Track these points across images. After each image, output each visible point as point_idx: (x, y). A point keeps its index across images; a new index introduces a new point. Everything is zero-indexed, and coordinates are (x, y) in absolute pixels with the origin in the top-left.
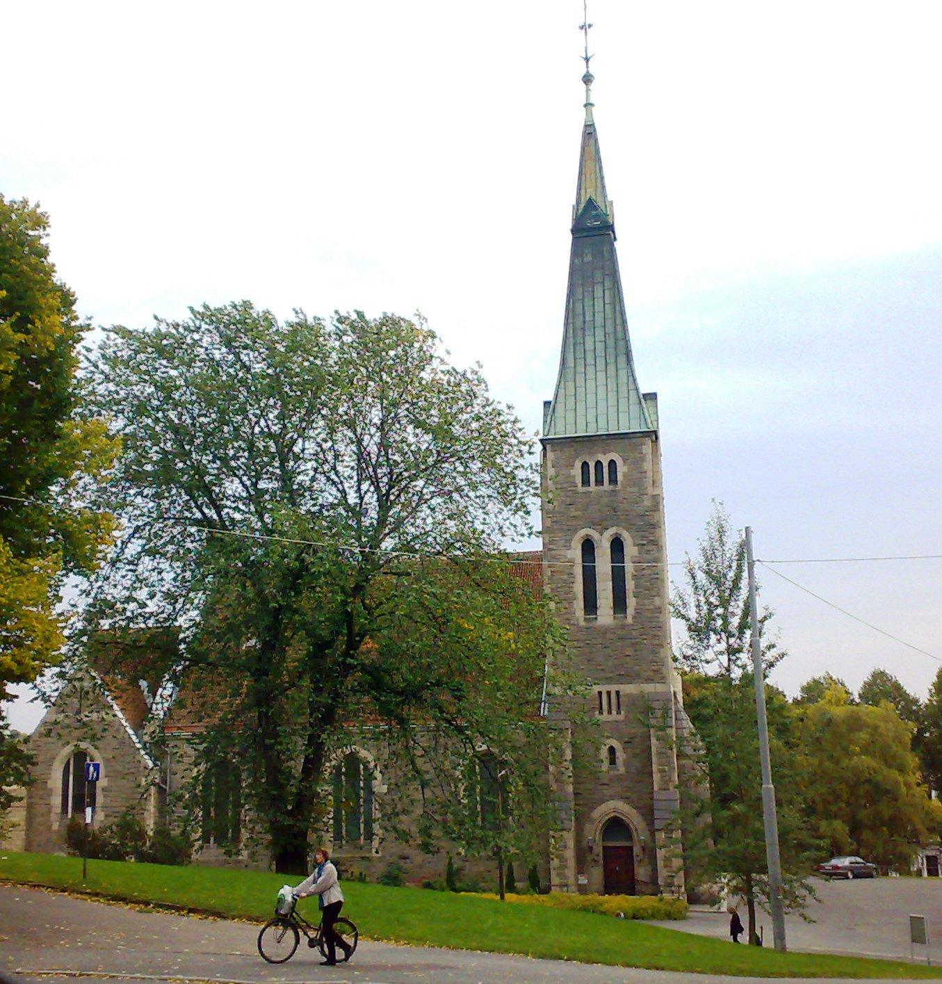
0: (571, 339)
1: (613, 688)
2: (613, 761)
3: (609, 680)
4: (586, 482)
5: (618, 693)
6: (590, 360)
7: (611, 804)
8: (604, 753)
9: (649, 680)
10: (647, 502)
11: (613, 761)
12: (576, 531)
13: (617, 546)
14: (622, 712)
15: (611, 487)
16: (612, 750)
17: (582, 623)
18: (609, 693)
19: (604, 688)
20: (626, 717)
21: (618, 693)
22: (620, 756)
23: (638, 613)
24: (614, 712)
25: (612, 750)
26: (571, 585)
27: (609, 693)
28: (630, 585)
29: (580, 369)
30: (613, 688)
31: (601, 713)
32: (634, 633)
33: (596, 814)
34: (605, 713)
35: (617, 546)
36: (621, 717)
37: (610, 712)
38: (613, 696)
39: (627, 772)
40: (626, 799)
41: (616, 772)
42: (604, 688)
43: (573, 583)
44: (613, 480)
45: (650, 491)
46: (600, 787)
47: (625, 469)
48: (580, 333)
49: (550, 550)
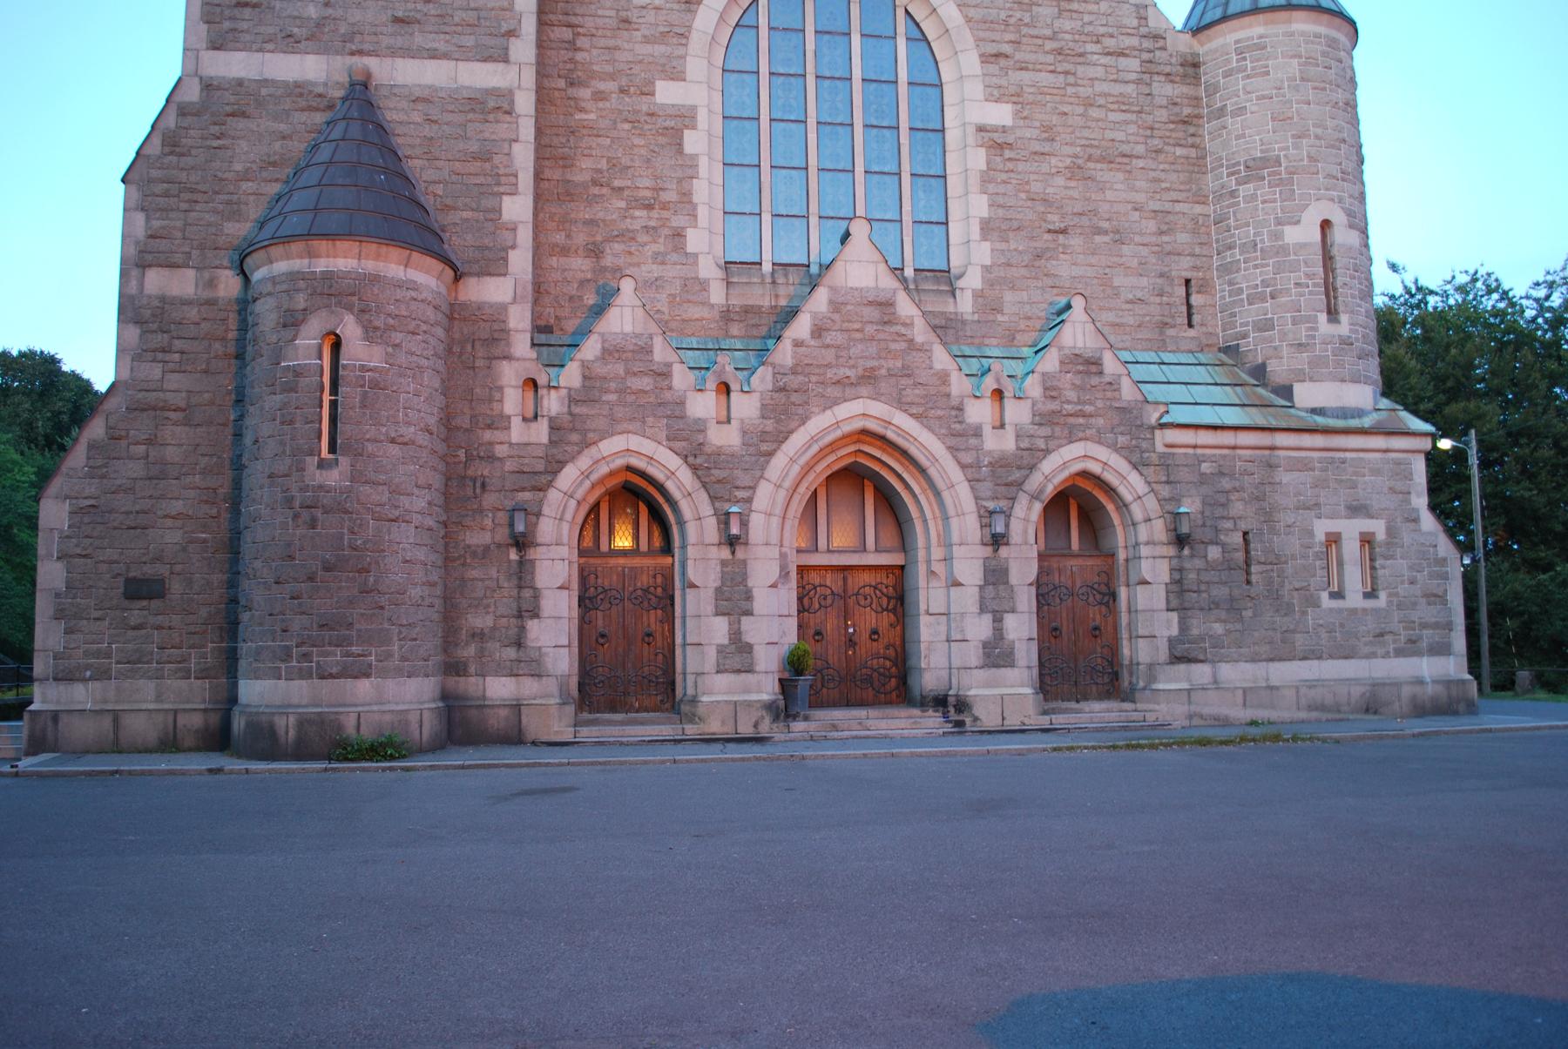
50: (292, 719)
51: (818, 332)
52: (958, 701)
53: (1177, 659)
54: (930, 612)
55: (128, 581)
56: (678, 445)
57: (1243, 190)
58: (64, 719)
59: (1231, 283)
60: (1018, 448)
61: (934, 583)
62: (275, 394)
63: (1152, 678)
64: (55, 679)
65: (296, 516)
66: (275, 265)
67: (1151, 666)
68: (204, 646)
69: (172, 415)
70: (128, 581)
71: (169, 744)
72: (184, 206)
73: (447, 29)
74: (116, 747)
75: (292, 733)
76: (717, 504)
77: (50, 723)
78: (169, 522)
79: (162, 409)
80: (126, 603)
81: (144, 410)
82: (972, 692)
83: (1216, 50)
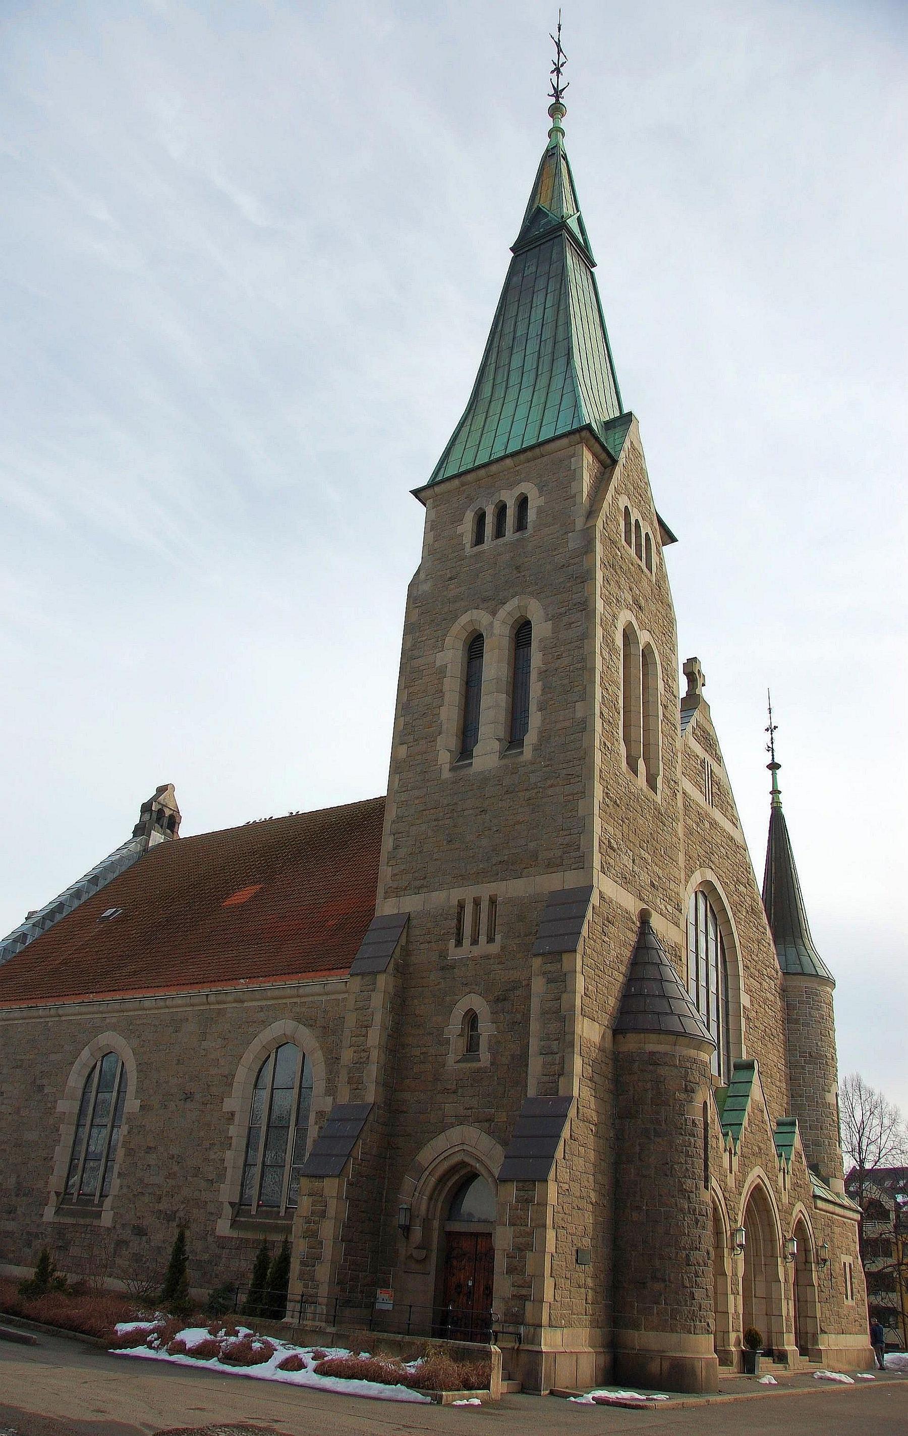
1: (485, 890)
2: (472, 1046)
3: (481, 876)
4: (479, 539)
7: (456, 1134)
8: (455, 1026)
9: (553, 866)
11: (472, 1046)
12: (456, 617)
14: (498, 937)
15: (518, 535)
16: (471, 1019)
17: (446, 774)
18: (477, 902)
19: (467, 893)
20: (503, 948)
22: (486, 1028)
23: (544, 737)
24: (483, 939)
25: (471, 1019)
27: (477, 902)
28: (535, 689)
29: (500, 393)
30: (485, 890)
31: (459, 943)
33: (426, 1156)
34: (467, 942)
36: (494, 948)
37: (475, 942)
38: (485, 905)
39: (492, 1064)
40: (486, 1122)
41: (475, 1065)
42: (467, 893)
44: (521, 525)
45: (579, 524)
47: (541, 501)
49: (413, 658)
54: (756, 1296)
57: (808, 1067)
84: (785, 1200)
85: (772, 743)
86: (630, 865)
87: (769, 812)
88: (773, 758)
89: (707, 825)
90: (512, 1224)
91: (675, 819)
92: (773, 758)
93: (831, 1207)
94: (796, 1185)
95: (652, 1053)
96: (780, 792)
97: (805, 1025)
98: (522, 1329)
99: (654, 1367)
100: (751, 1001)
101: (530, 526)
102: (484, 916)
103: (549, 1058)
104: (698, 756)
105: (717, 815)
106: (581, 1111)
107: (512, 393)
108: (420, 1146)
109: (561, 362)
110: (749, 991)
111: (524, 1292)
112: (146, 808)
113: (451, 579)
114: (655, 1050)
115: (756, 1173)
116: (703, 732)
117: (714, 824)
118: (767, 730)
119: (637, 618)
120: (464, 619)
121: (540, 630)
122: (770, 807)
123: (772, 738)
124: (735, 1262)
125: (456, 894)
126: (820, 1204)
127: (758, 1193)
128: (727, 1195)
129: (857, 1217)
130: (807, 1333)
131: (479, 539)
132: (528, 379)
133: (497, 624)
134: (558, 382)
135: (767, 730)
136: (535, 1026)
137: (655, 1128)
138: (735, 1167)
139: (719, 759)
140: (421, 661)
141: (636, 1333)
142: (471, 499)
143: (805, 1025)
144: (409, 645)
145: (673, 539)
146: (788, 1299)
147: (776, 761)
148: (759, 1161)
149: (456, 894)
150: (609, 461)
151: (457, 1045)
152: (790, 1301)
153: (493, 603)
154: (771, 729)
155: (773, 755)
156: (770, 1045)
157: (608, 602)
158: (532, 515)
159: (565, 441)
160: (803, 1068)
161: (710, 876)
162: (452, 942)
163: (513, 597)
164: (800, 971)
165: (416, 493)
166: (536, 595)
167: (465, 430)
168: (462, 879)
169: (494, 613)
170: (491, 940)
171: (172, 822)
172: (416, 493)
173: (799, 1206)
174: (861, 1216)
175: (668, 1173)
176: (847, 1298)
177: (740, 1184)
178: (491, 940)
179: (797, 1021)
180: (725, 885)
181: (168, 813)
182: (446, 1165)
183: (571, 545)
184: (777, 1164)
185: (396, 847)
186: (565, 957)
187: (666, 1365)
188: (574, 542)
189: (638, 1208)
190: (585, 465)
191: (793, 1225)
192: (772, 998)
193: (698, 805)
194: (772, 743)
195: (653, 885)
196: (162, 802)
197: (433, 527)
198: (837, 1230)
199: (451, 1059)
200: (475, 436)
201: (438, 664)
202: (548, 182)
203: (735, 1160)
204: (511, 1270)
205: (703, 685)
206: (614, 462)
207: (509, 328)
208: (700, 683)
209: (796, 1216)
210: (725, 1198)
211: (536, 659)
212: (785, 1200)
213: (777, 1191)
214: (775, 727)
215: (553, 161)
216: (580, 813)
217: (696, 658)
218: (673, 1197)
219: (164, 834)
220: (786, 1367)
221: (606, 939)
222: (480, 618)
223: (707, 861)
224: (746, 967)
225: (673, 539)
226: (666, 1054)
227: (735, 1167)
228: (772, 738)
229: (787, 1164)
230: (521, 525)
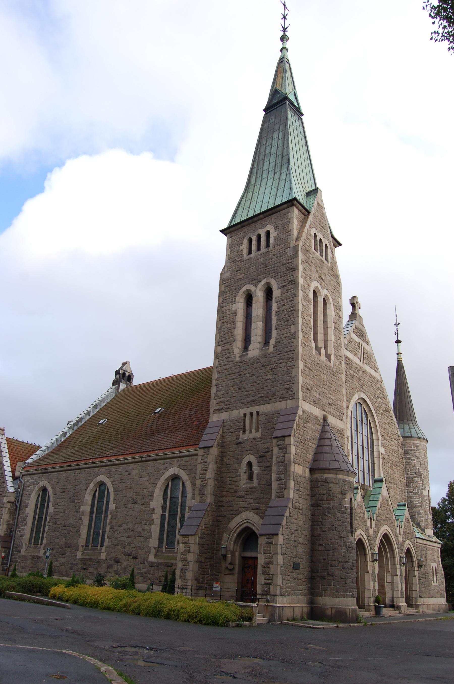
0: (256, 169)
2: (251, 477)
3: (253, 403)
4: (250, 252)
5: (258, 413)
6: (265, 175)
7: (245, 515)
8: (243, 468)
9: (282, 398)
10: (290, 252)
11: (251, 477)
12: (240, 288)
13: (269, 292)
15: (266, 250)
16: (250, 464)
17: (237, 359)
18: (251, 414)
19: (247, 411)
20: (262, 435)
21: (258, 413)
22: (256, 469)
23: (277, 342)
24: (254, 431)
25: (250, 464)
26: (233, 331)
27: (251, 414)
28: (274, 320)
29: (258, 182)
30: (254, 409)
31: (244, 432)
32: (274, 359)
33: (232, 525)
34: (247, 432)
35: (269, 292)
36: (258, 435)
37: (251, 431)
38: (254, 416)
39: (259, 484)
41: (251, 485)
42: (247, 411)
43: (234, 328)
44: (268, 245)
45: (293, 243)
46: (237, 500)
47: (275, 234)
48: (261, 163)
49: (222, 307)
50: (350, 610)
51: (381, 506)
52: (397, 606)
53: (420, 597)
55: (294, 563)
56: (367, 533)
57: (415, 479)
58: (285, 609)
59: (411, 501)
60: (402, 541)
61: (388, 574)
62: (340, 513)
63: (417, 602)
64: (281, 595)
65: (348, 550)
66: (338, 475)
67: (416, 598)
68: (305, 586)
69: (300, 511)
70: (294, 563)
71: (302, 619)
72: (301, 447)
73: (336, 409)
74: (294, 619)
75: (350, 614)
76: (372, 550)
77: (282, 611)
78: (300, 545)
79: (298, 509)
80: (293, 571)
81: (296, 508)
82: (400, 604)
83: (408, 443)
84: (400, 539)
85: (397, 331)
86: (317, 396)
87: (396, 363)
88: (398, 338)
89: (361, 373)
90: (264, 553)
91: (342, 374)
92: (398, 338)
93: (425, 542)
94: (405, 533)
95: (326, 479)
96: (401, 354)
97: (413, 460)
98: (269, 597)
99: (329, 612)
100: (385, 451)
101: (271, 245)
102: (254, 421)
103: (280, 482)
104: (356, 342)
105: (367, 368)
106: (294, 504)
107: (264, 181)
108: (230, 519)
109: (285, 166)
110: (384, 446)
111: (269, 581)
112: (117, 373)
113: (238, 271)
114: (328, 477)
115: (384, 529)
116: (359, 330)
117: (365, 372)
118: (395, 325)
119: (321, 284)
120: (244, 289)
121: (276, 293)
122: (397, 360)
123: (397, 329)
124: (373, 567)
125: (243, 411)
126: (418, 540)
127: (386, 536)
128: (369, 538)
129: (440, 546)
130: (413, 598)
131: (250, 252)
132: (271, 174)
133: (257, 291)
134: (283, 176)
135: (395, 325)
136: (274, 468)
137: (328, 511)
138: (373, 525)
139: (367, 342)
140: (226, 308)
141: (321, 598)
142: (246, 234)
143: (413, 460)
144: (221, 301)
145: (340, 245)
146: (402, 583)
147: (399, 339)
148: (386, 523)
149: (243, 411)
150: (306, 213)
151: (245, 477)
152: (403, 584)
153: (255, 281)
154: (397, 324)
155: (398, 337)
156: (395, 470)
157: (305, 279)
158: (272, 240)
159: (286, 205)
160: (412, 479)
161: (363, 395)
162: (241, 432)
163: (264, 278)
164: (410, 435)
165: (222, 231)
166: (274, 277)
167: (244, 200)
168: (245, 405)
169: (256, 286)
170: (257, 431)
171: (129, 378)
172: (222, 231)
173: (408, 542)
174: (442, 546)
175: (334, 530)
176: (434, 582)
177: (376, 533)
178: (257, 431)
179: (409, 459)
180: (370, 399)
181: (127, 374)
182: (240, 528)
183: (289, 254)
184: (396, 524)
185: (217, 391)
186: (287, 439)
187: (334, 611)
188: (290, 252)
189: (322, 545)
190: (294, 216)
191: (405, 550)
192: (396, 449)
193: (356, 364)
194: (397, 331)
195: (329, 404)
196: (124, 370)
197: (230, 247)
198: (428, 552)
199: (242, 483)
200: (248, 203)
201: (233, 309)
202: (280, 75)
203: (373, 523)
204: (264, 573)
205: (359, 308)
206: (309, 212)
207: (263, 150)
208: (357, 307)
209: (406, 546)
210: (368, 540)
211: (275, 306)
212: (400, 539)
213: (396, 536)
214: (399, 324)
215: (282, 64)
216: (293, 375)
217: (355, 296)
218: (336, 540)
219: (126, 384)
220: (400, 612)
221: (305, 429)
222: (251, 287)
223: (362, 389)
224: (382, 436)
225: (340, 245)
226: (333, 478)
227: (373, 525)
228: (397, 329)
229: (401, 523)
230: (268, 245)
